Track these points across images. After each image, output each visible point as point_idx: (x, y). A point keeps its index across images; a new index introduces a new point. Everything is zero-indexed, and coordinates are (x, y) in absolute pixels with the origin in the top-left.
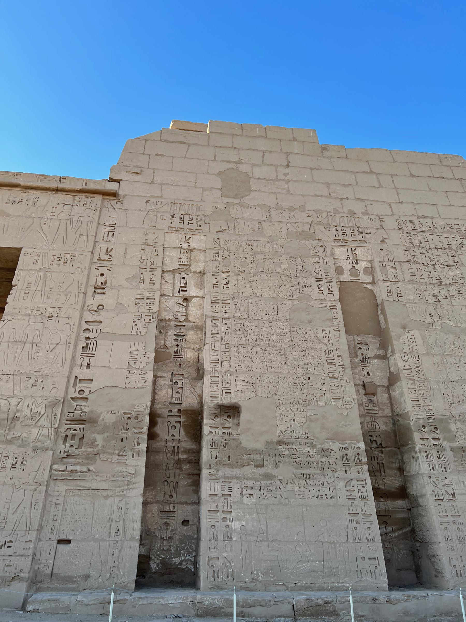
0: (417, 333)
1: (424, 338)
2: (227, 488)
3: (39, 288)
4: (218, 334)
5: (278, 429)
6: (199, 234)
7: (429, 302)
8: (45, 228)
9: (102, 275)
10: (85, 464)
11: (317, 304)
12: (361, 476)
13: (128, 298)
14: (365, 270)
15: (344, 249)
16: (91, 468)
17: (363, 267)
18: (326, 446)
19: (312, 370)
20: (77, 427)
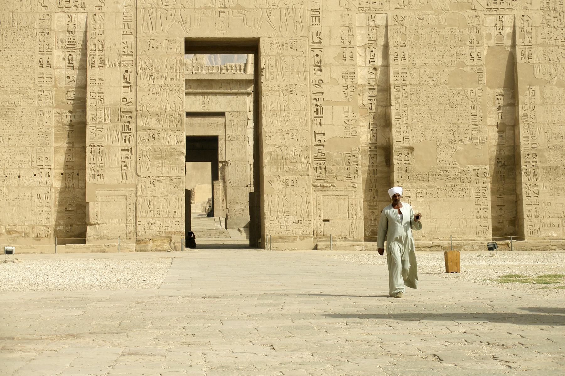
0: (537, 88)
1: (542, 92)
2: (408, 193)
3: (279, 70)
4: (398, 98)
5: (438, 160)
6: (382, 12)
7: (551, 62)
8: (271, 17)
9: (317, 55)
10: (330, 183)
11: (468, 69)
12: (485, 185)
13: (337, 73)
14: (508, 34)
15: (492, 18)
16: (333, 184)
17: (507, 32)
18: (465, 169)
19: (461, 121)
20: (321, 162)
